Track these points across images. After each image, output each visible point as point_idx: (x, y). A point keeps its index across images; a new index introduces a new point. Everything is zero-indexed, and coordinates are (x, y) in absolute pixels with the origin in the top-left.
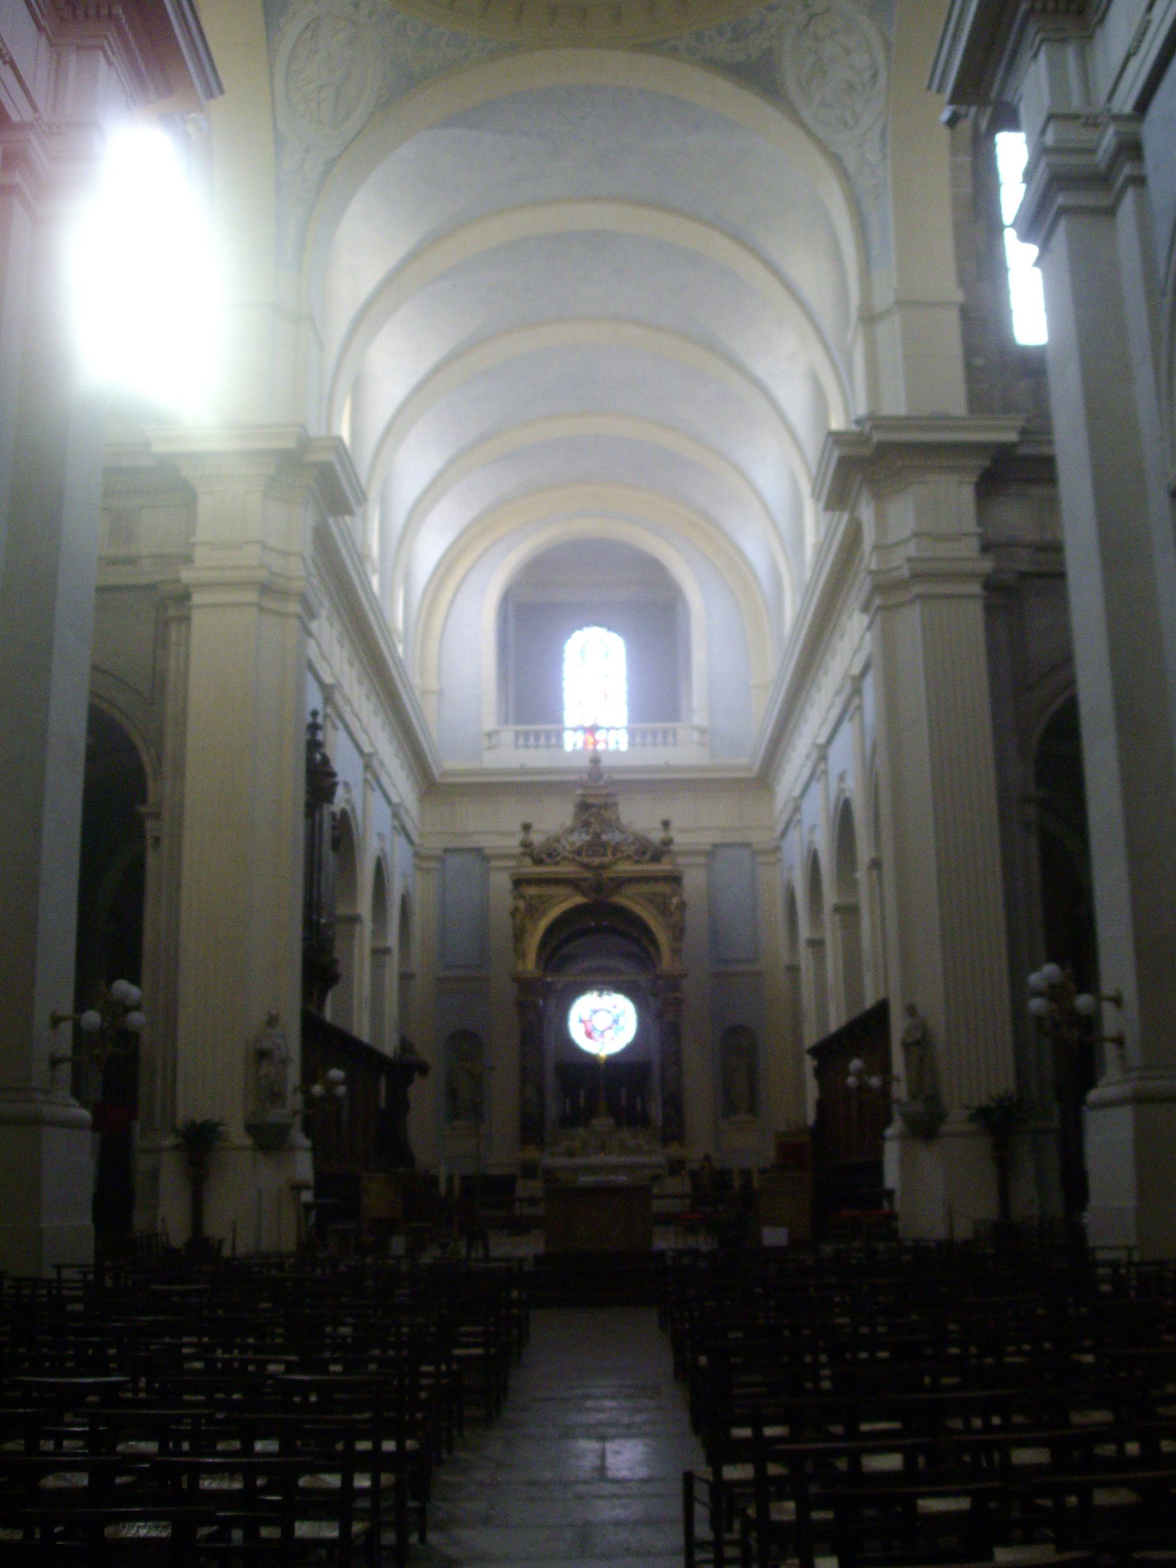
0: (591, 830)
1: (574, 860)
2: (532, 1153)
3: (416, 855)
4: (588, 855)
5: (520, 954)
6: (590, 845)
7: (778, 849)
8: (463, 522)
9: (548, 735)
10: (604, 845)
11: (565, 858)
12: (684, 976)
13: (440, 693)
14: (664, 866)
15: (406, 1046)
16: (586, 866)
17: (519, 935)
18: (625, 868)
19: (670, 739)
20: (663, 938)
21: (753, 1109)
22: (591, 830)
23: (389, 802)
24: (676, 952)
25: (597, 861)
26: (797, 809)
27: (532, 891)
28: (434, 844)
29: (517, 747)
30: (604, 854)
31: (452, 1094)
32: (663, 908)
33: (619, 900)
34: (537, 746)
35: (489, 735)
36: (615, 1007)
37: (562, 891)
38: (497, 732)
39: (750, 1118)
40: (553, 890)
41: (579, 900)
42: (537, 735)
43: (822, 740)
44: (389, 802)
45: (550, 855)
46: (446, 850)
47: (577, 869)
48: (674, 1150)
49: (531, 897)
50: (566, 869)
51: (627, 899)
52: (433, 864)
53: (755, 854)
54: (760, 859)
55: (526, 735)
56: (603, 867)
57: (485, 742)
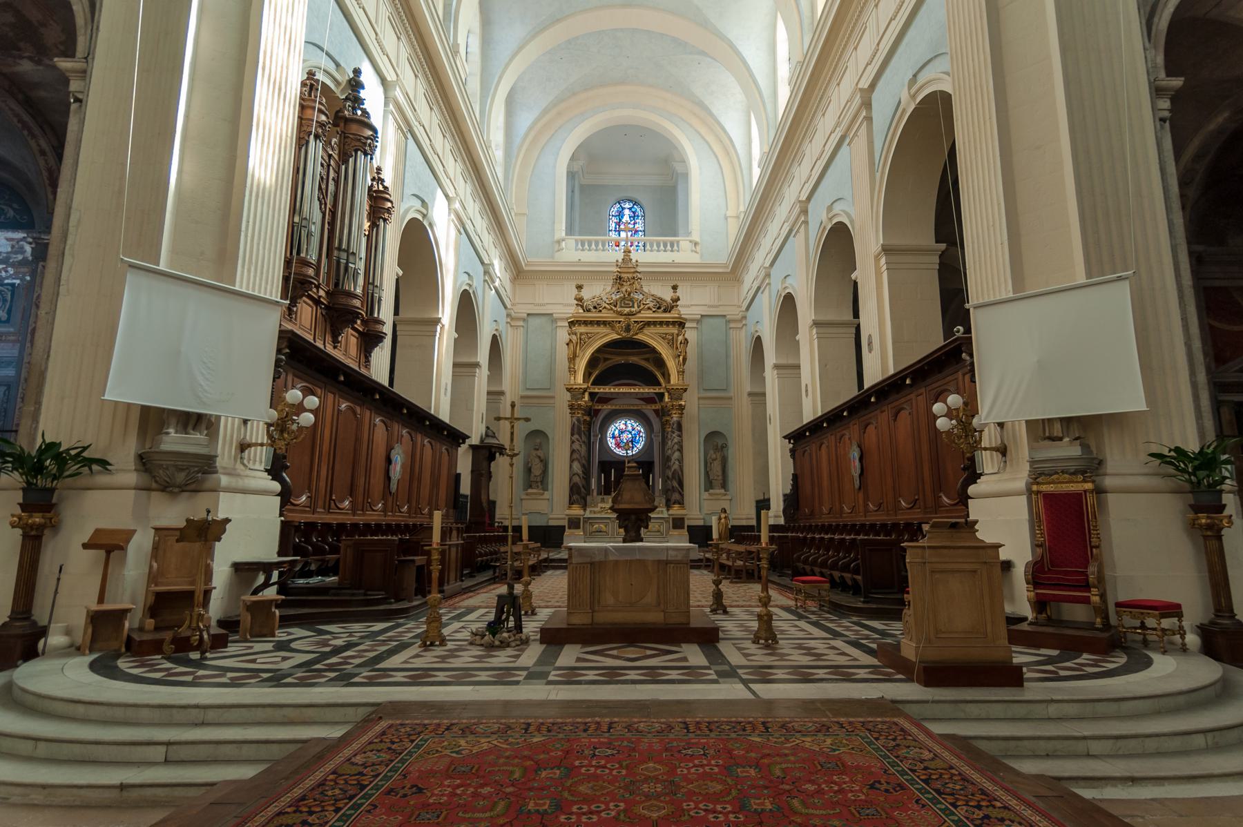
0: (624, 290)
1: (612, 309)
2: (576, 511)
3: (508, 315)
4: (621, 307)
5: (573, 371)
6: (624, 298)
7: (744, 317)
9: (597, 244)
10: (631, 300)
11: (605, 307)
12: (685, 390)
14: (672, 315)
15: (489, 433)
16: (621, 314)
17: (572, 359)
18: (647, 315)
20: (671, 364)
21: (724, 485)
22: (624, 290)
23: (482, 263)
24: (681, 373)
25: (627, 310)
26: (768, 275)
27: (583, 329)
28: (522, 310)
30: (633, 307)
31: (528, 470)
32: (671, 342)
33: (640, 337)
34: (590, 250)
35: (559, 242)
36: (633, 429)
37: (602, 330)
39: (722, 491)
40: (595, 329)
41: (615, 336)
43: (803, 197)
44: (482, 263)
45: (595, 308)
46: (528, 315)
47: (615, 315)
48: (676, 511)
49: (581, 334)
50: (606, 315)
51: (649, 337)
52: (521, 323)
53: (729, 322)
54: (732, 325)
56: (631, 314)
57: (556, 247)
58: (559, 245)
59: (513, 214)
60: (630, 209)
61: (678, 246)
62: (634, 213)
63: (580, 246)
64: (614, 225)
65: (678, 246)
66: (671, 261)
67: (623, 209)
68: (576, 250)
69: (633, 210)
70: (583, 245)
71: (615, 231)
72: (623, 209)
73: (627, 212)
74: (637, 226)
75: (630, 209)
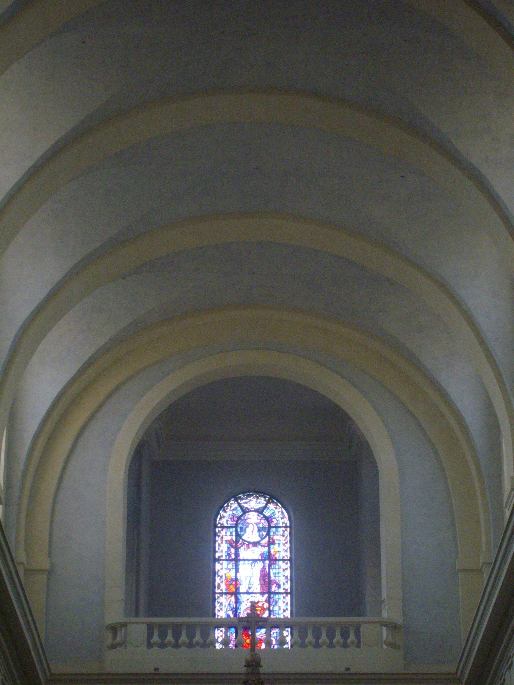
8: (88, 353)
13: (50, 573)
19: (352, 638)
29: (150, 645)
34: (177, 645)
35: (114, 629)
38: (124, 625)
42: (177, 630)
55: (163, 629)
57: (109, 639)
58: (115, 636)
59: (21, 572)
60: (260, 511)
61: (358, 636)
62: (269, 519)
63: (156, 638)
64: (224, 547)
65: (358, 636)
66: (341, 669)
67: (245, 511)
68: (150, 645)
69: (267, 513)
70: (163, 635)
71: (229, 560)
72: (245, 511)
73: (253, 518)
74: (274, 549)
75: (260, 511)
